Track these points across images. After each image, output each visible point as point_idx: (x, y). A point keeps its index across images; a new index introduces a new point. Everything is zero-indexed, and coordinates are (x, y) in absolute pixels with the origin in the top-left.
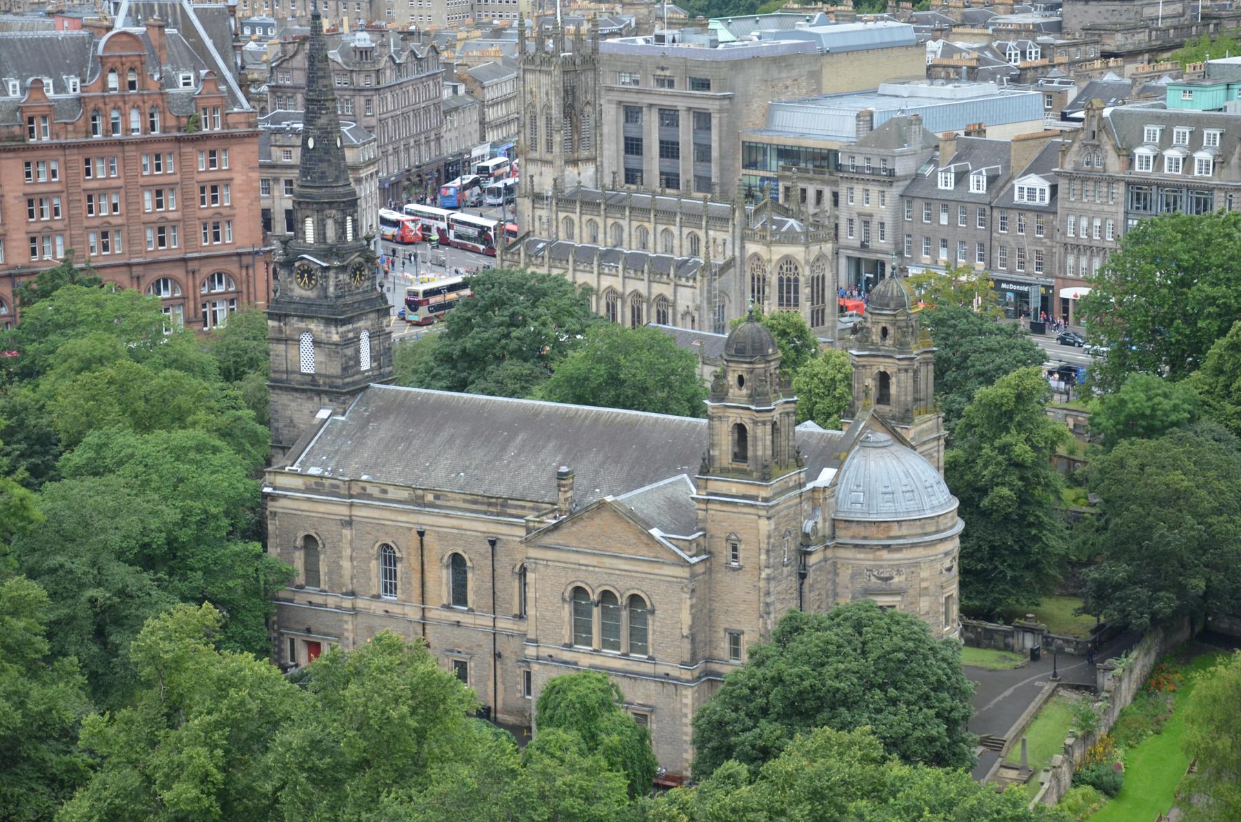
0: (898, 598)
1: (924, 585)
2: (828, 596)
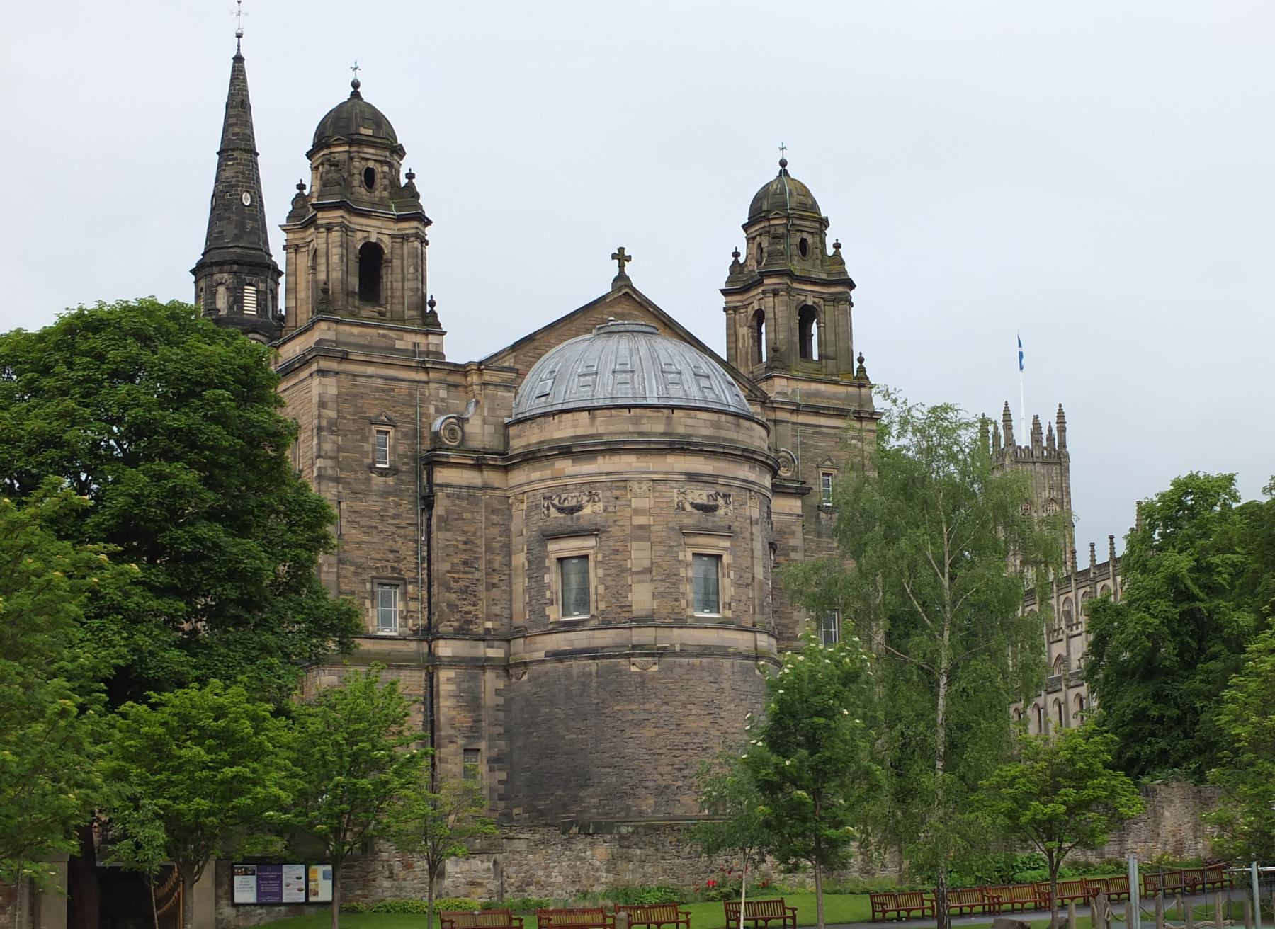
0: (591, 542)
1: (640, 520)
2: (489, 549)
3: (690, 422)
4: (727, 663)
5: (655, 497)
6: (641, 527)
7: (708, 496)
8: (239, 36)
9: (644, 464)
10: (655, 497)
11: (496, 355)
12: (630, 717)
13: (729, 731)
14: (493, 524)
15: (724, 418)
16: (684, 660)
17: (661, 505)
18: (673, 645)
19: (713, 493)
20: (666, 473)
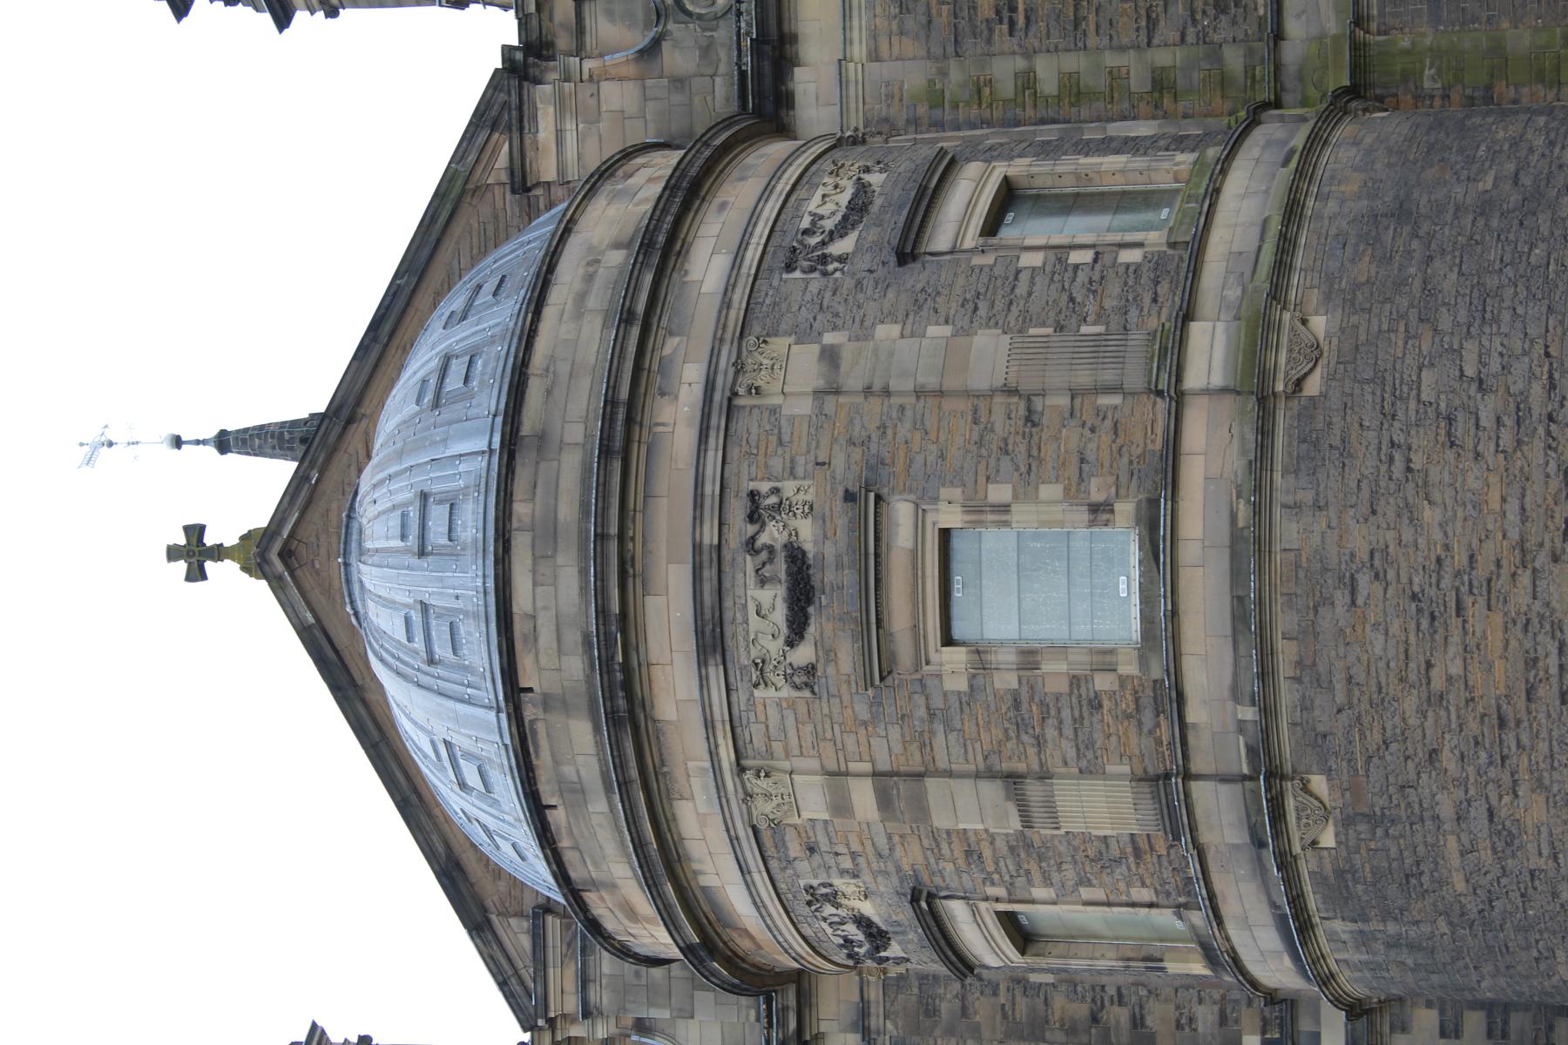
0: (957, 912)
3: (546, 637)
4: (1288, 532)
5: (787, 756)
6: (885, 802)
7: (763, 582)
8: (178, 442)
9: (696, 783)
10: (787, 756)
11: (503, 985)
12: (1486, 856)
13: (1514, 534)
14: (964, 1012)
15: (521, 509)
16: (1287, 695)
17: (808, 739)
18: (1241, 726)
19: (750, 563)
20: (709, 725)
